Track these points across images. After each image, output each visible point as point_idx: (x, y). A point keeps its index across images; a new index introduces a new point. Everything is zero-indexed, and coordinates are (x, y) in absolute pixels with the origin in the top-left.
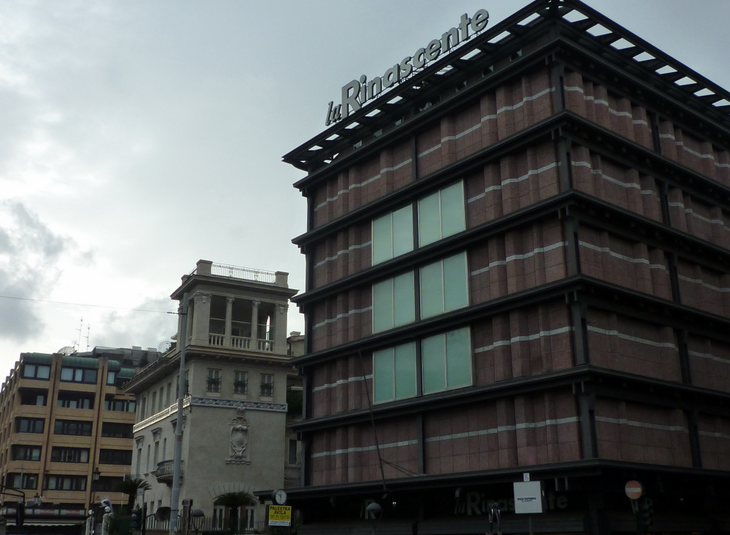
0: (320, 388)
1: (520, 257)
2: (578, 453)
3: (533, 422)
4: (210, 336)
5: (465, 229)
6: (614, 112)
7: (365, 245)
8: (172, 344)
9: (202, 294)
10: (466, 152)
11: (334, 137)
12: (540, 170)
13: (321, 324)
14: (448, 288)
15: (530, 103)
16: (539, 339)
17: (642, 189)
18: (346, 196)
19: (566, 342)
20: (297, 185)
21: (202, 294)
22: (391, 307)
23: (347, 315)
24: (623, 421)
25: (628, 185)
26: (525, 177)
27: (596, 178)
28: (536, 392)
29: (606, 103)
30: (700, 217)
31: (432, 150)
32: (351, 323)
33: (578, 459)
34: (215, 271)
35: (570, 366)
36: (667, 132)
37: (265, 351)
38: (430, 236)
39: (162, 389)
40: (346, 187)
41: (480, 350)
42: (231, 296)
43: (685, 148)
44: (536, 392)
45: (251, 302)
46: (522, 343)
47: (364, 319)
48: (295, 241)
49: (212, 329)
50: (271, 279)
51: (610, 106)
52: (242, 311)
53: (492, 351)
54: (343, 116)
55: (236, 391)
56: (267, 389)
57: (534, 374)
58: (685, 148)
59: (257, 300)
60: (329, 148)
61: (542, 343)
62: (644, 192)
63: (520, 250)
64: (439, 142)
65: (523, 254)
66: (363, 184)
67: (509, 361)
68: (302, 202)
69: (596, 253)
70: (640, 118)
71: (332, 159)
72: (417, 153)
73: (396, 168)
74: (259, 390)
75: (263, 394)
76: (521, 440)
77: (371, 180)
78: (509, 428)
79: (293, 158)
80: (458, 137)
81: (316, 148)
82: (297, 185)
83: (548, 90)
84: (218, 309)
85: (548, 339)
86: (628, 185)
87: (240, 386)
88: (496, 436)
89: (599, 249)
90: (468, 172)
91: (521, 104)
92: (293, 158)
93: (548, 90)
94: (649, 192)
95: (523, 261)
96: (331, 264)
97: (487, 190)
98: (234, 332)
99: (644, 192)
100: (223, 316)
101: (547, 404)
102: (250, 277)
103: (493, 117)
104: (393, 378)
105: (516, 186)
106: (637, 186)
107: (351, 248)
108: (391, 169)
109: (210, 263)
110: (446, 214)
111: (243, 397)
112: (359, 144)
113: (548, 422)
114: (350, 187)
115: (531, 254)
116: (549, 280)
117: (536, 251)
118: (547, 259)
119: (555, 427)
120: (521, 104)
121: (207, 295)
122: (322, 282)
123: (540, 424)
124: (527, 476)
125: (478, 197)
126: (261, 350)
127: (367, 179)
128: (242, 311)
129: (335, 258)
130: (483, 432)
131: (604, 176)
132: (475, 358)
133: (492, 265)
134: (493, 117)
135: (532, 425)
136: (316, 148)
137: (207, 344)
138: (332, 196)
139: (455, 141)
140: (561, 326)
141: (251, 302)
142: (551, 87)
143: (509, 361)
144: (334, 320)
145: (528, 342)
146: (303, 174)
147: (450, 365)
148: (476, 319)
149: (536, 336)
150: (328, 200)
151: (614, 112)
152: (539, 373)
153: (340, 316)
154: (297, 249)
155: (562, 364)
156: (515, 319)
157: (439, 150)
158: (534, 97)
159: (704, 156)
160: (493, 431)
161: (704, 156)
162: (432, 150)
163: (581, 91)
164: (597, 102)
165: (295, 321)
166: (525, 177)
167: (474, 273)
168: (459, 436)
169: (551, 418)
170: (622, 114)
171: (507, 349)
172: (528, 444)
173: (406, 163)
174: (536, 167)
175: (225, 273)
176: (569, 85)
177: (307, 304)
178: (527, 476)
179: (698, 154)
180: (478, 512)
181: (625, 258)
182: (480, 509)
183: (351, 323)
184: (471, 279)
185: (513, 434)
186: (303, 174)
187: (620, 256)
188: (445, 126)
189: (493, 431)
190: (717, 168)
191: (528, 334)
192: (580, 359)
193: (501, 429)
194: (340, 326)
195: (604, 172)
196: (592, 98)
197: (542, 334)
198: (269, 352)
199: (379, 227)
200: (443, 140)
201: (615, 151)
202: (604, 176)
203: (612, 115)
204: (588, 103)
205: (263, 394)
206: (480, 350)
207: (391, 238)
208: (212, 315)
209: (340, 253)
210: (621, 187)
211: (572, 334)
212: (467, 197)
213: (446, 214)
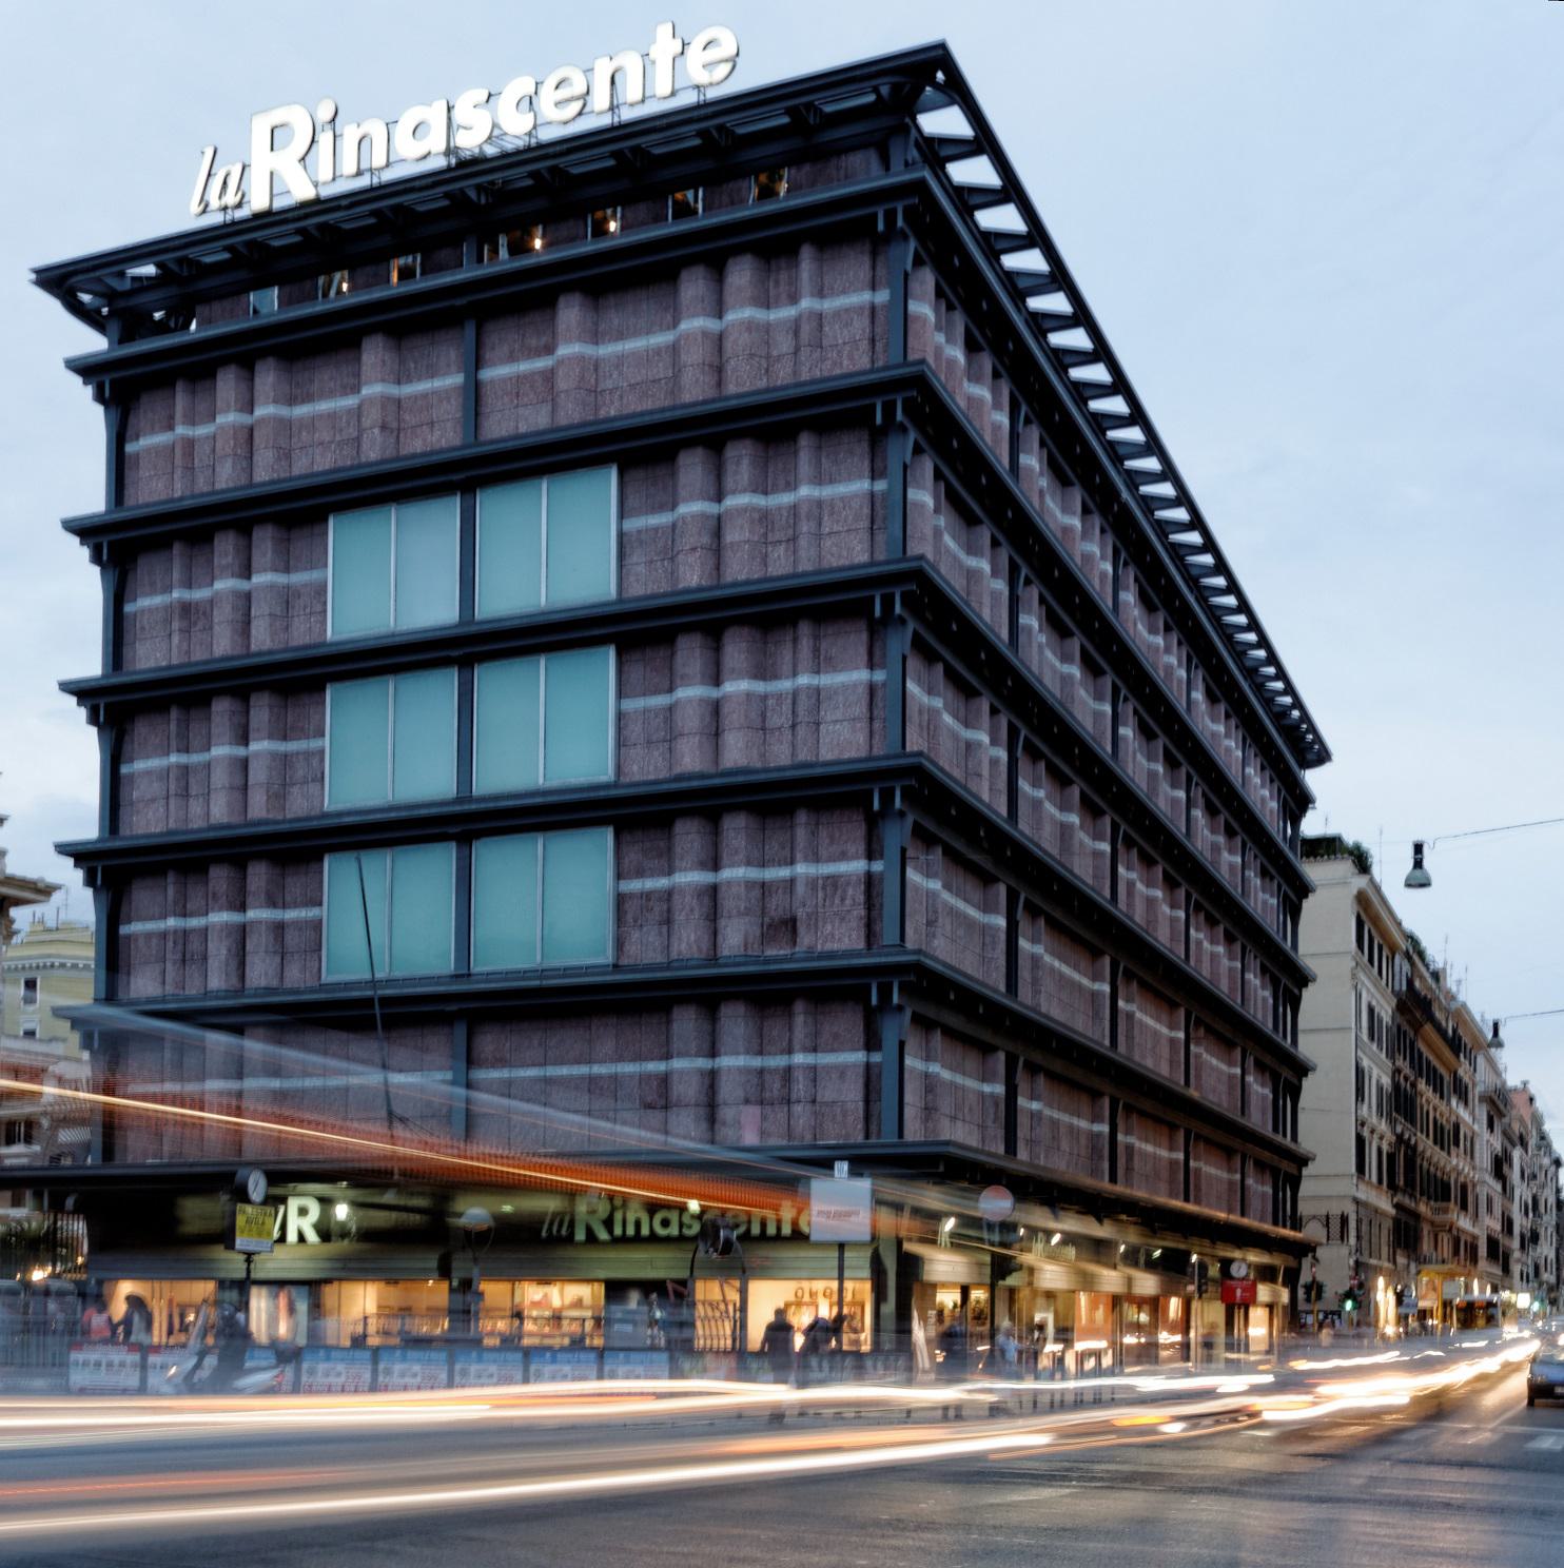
1: (760, 687)
2: (860, 1126)
3: (761, 1053)
5: (612, 592)
10: (624, 404)
14: (559, 729)
19: (857, 894)
24: (934, 1068)
28: (774, 993)
31: (524, 367)
33: (860, 1139)
35: (861, 945)
41: (634, 886)
44: (774, 993)
53: (668, 895)
57: (771, 952)
61: (800, 889)
63: (762, 672)
64: (549, 350)
67: (713, 916)
72: (479, 363)
76: (728, 1090)
78: (703, 1063)
85: (813, 883)
88: (665, 1080)
95: (764, 698)
101: (799, 1019)
104: (387, 923)
113: (799, 1058)
116: (827, 754)
118: (827, 703)
119: (814, 1068)
123: (777, 1062)
124: (842, 1168)
130: (628, 1068)
132: (621, 900)
133: (682, 693)
135: (757, 1062)
140: (843, 856)
143: (713, 916)
147: (553, 909)
148: (635, 816)
149: (784, 873)
152: (774, 952)
155: (837, 937)
156: (736, 829)
160: (655, 1067)
162: (524, 367)
167: (630, 705)
168: (564, 1071)
169: (805, 1050)
171: (713, 891)
172: (747, 1101)
178: (842, 1168)
180: (603, 1235)
182: (610, 1230)
185: (712, 1078)
188: (570, 313)
189: (655, 1067)
192: (889, 935)
193: (678, 1064)
197: (802, 869)
206: (634, 886)
211: (870, 880)
212: (622, 515)
213: (561, 547)
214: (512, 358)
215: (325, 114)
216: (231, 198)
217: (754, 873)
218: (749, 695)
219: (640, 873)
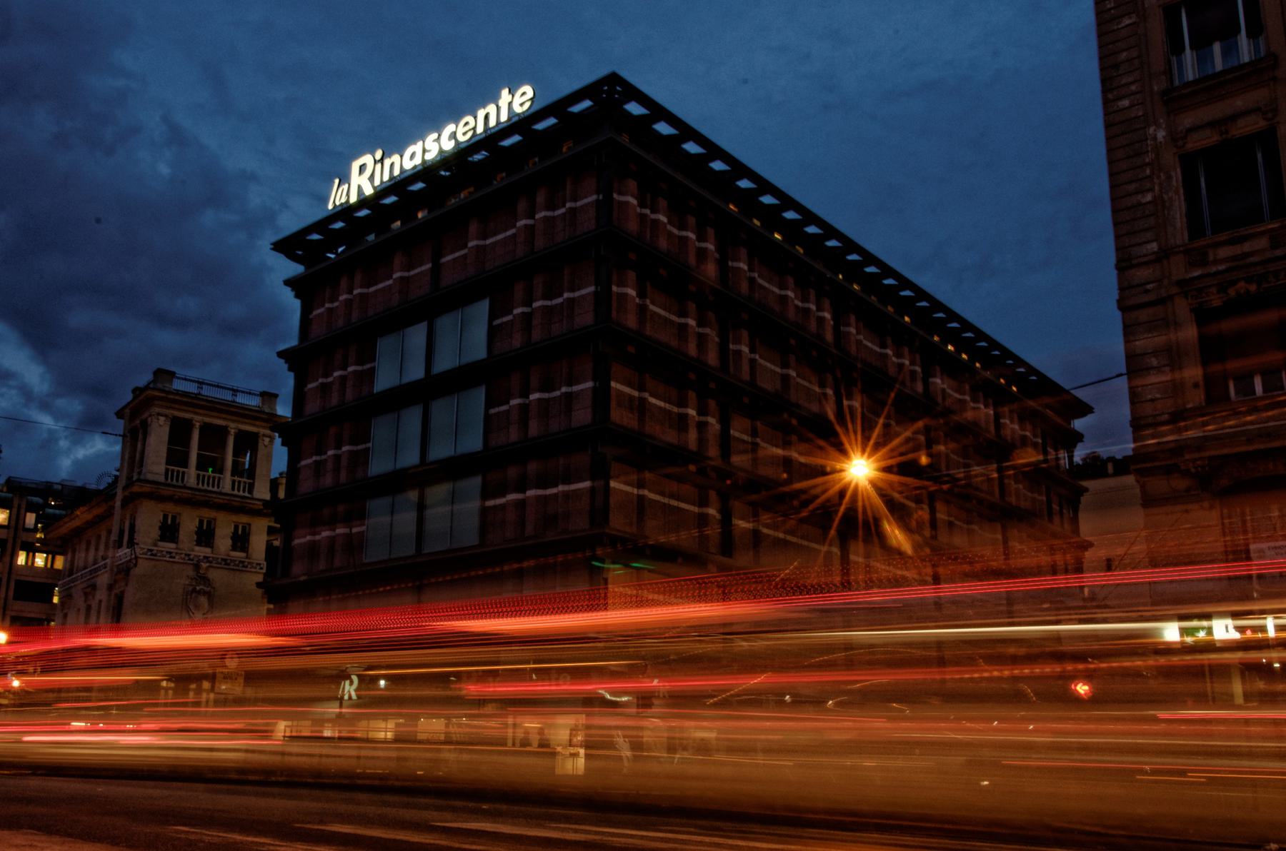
0: (303, 540)
1: (546, 396)
4: (167, 470)
6: (676, 231)
7: (368, 366)
8: (116, 477)
9: (159, 414)
11: (339, 225)
12: (577, 294)
13: (309, 461)
14: (463, 427)
15: (573, 210)
16: (555, 495)
17: (699, 325)
18: (348, 303)
20: (288, 283)
21: (159, 414)
22: (396, 446)
23: (339, 452)
25: (682, 320)
26: (560, 300)
27: (642, 309)
29: (664, 219)
30: (768, 365)
31: (457, 254)
32: (344, 462)
34: (178, 385)
36: (739, 260)
37: (241, 493)
38: (444, 363)
39: (99, 537)
40: (350, 292)
42: (198, 419)
43: (760, 281)
45: (224, 431)
46: (538, 497)
47: (361, 459)
48: (281, 354)
49: (169, 461)
50: (253, 402)
51: (670, 222)
52: (214, 437)
54: (353, 199)
55: (199, 543)
56: (241, 540)
58: (760, 281)
59: (233, 427)
60: (332, 239)
62: (701, 330)
63: (546, 386)
64: (465, 246)
65: (549, 391)
66: (372, 289)
68: (297, 303)
69: (631, 398)
70: (705, 240)
71: (336, 253)
73: (412, 273)
74: (156, 533)
75: (234, 548)
77: (380, 286)
79: (286, 246)
80: (488, 242)
81: (315, 237)
82: (288, 283)
83: (595, 197)
84: (179, 432)
85: (566, 495)
86: (682, 320)
87: (205, 536)
89: (636, 394)
90: (495, 285)
91: (562, 210)
92: (286, 246)
93: (595, 197)
94: (707, 331)
95: (548, 400)
96: (325, 388)
97: (516, 311)
98: (201, 466)
99: (701, 330)
100: (187, 445)
102: (227, 396)
103: (530, 222)
105: (548, 311)
106: (692, 322)
107: (351, 369)
108: (406, 274)
109: (172, 375)
110: (468, 336)
111: (205, 551)
112: (371, 237)
114: (356, 292)
115: (557, 393)
117: (564, 389)
120: (562, 210)
121: (166, 416)
122: (312, 407)
125: (505, 319)
126: (236, 492)
127: (376, 284)
128: (214, 437)
129: (330, 379)
131: (652, 307)
133: (514, 402)
134: (530, 222)
136: (315, 237)
137: (162, 479)
138: (332, 302)
139: (485, 246)
140: (581, 480)
141: (224, 431)
142: (598, 193)
144: (324, 457)
145: (546, 497)
146: (296, 269)
150: (327, 305)
151: (676, 231)
153: (330, 453)
154: (282, 365)
157: (465, 256)
158: (579, 204)
159: (783, 293)
161: (783, 293)
162: (457, 254)
163: (634, 202)
164: (653, 216)
165: (277, 458)
166: (560, 300)
167: (492, 411)
170: (684, 233)
173: (424, 268)
174: (573, 290)
175: (192, 388)
176: (620, 193)
177: (292, 433)
179: (776, 290)
181: (668, 406)
183: (344, 462)
184: (488, 418)
186: (296, 269)
187: (661, 404)
190: (797, 307)
191: (545, 488)
194: (330, 465)
195: (653, 303)
196: (648, 211)
197: (561, 488)
198: (247, 494)
199: (385, 345)
200: (471, 244)
201: (670, 278)
202: (652, 307)
203: (670, 234)
204: (643, 216)
205: (234, 548)
207: (401, 361)
208: (170, 442)
209: (336, 374)
210: (672, 322)
213: (468, 336)
214: (452, 252)
215: (379, 154)
216: (343, 200)
217: (540, 492)
218: (539, 400)
219: (494, 497)
